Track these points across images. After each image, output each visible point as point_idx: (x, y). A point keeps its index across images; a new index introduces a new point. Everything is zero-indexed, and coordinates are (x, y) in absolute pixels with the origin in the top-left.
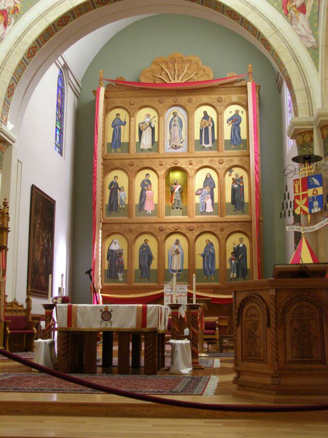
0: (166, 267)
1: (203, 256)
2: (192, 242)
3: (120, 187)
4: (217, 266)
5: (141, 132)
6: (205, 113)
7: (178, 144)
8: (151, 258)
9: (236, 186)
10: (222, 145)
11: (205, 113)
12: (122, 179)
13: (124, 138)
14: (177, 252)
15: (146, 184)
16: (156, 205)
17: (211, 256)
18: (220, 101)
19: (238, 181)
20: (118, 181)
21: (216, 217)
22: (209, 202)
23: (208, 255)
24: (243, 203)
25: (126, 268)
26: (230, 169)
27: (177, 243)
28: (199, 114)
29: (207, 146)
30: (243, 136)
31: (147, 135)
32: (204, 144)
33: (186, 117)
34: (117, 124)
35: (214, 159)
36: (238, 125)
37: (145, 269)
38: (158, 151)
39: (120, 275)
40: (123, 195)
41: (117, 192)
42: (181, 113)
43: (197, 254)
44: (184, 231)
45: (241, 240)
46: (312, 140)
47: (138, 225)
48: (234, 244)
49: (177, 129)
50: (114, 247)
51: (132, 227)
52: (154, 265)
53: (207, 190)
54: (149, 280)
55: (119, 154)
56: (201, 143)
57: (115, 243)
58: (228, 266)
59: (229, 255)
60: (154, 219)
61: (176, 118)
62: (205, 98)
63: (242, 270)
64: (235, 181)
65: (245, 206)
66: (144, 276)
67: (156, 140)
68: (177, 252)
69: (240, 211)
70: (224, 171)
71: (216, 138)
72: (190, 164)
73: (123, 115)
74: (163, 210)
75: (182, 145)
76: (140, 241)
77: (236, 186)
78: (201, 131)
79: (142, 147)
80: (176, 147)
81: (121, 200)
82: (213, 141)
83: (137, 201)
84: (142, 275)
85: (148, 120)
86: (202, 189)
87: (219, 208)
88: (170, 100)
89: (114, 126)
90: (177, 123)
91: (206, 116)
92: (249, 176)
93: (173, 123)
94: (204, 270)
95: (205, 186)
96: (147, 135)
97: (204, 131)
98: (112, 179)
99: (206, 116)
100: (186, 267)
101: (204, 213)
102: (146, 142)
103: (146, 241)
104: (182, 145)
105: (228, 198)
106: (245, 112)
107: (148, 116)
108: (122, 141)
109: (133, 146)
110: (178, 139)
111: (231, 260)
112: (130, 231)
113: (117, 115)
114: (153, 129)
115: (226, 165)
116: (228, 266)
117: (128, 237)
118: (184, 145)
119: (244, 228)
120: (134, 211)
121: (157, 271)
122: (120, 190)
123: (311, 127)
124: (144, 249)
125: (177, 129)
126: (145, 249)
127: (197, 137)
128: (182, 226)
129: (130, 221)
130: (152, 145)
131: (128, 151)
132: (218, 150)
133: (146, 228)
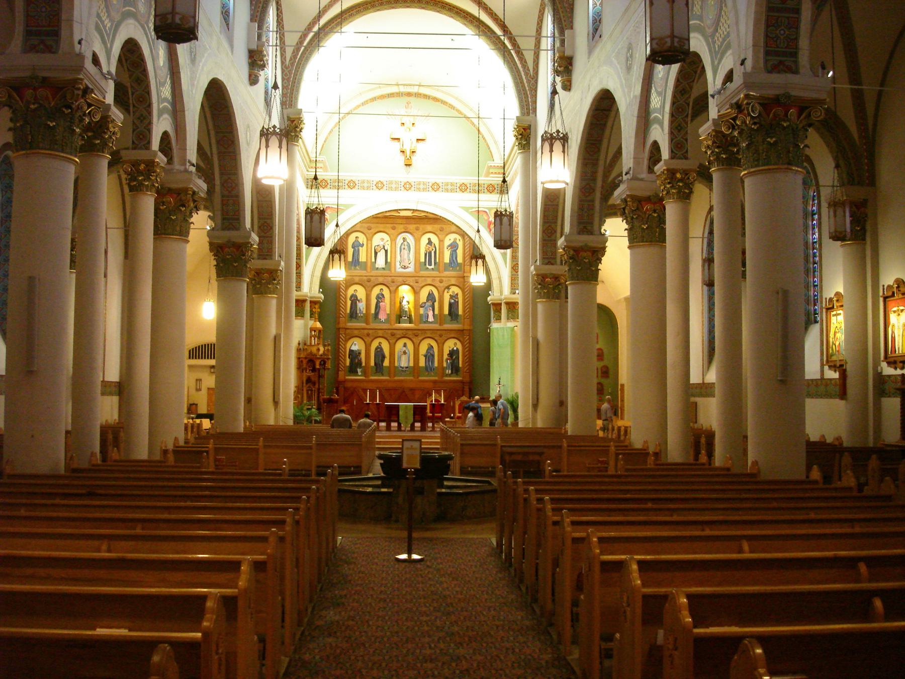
0: (396, 364)
1: (425, 356)
2: (416, 346)
3: (359, 298)
4: (436, 364)
5: (376, 253)
6: (429, 239)
7: (407, 265)
8: (384, 357)
9: (453, 301)
10: (442, 267)
11: (429, 239)
13: (363, 258)
14: (405, 353)
15: (380, 297)
16: (388, 314)
17: (431, 357)
18: (442, 230)
19: (454, 297)
20: (357, 294)
21: (437, 326)
22: (431, 313)
23: (429, 356)
24: (457, 315)
25: (364, 364)
26: (448, 288)
27: (405, 345)
28: (424, 240)
29: (430, 267)
30: (460, 260)
31: (381, 256)
32: (428, 266)
33: (413, 242)
34: (357, 246)
35: (436, 279)
36: (455, 251)
37: (379, 366)
38: (390, 270)
39: (359, 370)
40: (361, 306)
41: (356, 303)
43: (420, 354)
44: (410, 337)
45: (455, 344)
46: (501, 309)
47: (374, 331)
48: (450, 347)
49: (405, 252)
50: (354, 348)
51: (371, 332)
52: (386, 363)
53: (430, 303)
54: (383, 375)
56: (426, 265)
57: (355, 344)
58: (445, 365)
59: (445, 356)
61: (405, 243)
62: (429, 228)
63: (455, 369)
64: (451, 297)
65: (459, 318)
66: (378, 371)
67: (389, 260)
68: (405, 353)
69: (455, 322)
70: (443, 289)
71: (437, 261)
72: (417, 282)
73: (362, 239)
74: (393, 318)
75: (410, 265)
76: (375, 345)
77: (453, 301)
78: (426, 255)
79: (377, 266)
80: (405, 268)
81: (360, 310)
82: (435, 263)
83: (373, 311)
84: (376, 370)
85: (381, 243)
86: (425, 303)
87: (439, 318)
88: (400, 228)
89: (353, 247)
90: (406, 247)
91: (430, 242)
93: (403, 247)
94: (426, 368)
95: (428, 300)
96: (381, 256)
97: (428, 255)
98: (353, 292)
99: (430, 242)
100: (411, 364)
101: (427, 322)
102: (381, 262)
103: (380, 343)
104: (410, 265)
105: (446, 311)
106: (461, 240)
107: (382, 239)
108: (360, 260)
109: (369, 264)
110: (407, 261)
111: (447, 359)
112: (368, 335)
113: (356, 237)
114: (386, 251)
115: (445, 284)
116: (445, 365)
117: (366, 340)
119: (459, 334)
120: (371, 319)
121: (389, 367)
122: (359, 301)
123: (500, 302)
124: (379, 350)
125: (405, 252)
127: (422, 260)
128: (410, 332)
129: (368, 327)
130: (386, 264)
131: (366, 269)
132: (439, 271)
133: (380, 333)
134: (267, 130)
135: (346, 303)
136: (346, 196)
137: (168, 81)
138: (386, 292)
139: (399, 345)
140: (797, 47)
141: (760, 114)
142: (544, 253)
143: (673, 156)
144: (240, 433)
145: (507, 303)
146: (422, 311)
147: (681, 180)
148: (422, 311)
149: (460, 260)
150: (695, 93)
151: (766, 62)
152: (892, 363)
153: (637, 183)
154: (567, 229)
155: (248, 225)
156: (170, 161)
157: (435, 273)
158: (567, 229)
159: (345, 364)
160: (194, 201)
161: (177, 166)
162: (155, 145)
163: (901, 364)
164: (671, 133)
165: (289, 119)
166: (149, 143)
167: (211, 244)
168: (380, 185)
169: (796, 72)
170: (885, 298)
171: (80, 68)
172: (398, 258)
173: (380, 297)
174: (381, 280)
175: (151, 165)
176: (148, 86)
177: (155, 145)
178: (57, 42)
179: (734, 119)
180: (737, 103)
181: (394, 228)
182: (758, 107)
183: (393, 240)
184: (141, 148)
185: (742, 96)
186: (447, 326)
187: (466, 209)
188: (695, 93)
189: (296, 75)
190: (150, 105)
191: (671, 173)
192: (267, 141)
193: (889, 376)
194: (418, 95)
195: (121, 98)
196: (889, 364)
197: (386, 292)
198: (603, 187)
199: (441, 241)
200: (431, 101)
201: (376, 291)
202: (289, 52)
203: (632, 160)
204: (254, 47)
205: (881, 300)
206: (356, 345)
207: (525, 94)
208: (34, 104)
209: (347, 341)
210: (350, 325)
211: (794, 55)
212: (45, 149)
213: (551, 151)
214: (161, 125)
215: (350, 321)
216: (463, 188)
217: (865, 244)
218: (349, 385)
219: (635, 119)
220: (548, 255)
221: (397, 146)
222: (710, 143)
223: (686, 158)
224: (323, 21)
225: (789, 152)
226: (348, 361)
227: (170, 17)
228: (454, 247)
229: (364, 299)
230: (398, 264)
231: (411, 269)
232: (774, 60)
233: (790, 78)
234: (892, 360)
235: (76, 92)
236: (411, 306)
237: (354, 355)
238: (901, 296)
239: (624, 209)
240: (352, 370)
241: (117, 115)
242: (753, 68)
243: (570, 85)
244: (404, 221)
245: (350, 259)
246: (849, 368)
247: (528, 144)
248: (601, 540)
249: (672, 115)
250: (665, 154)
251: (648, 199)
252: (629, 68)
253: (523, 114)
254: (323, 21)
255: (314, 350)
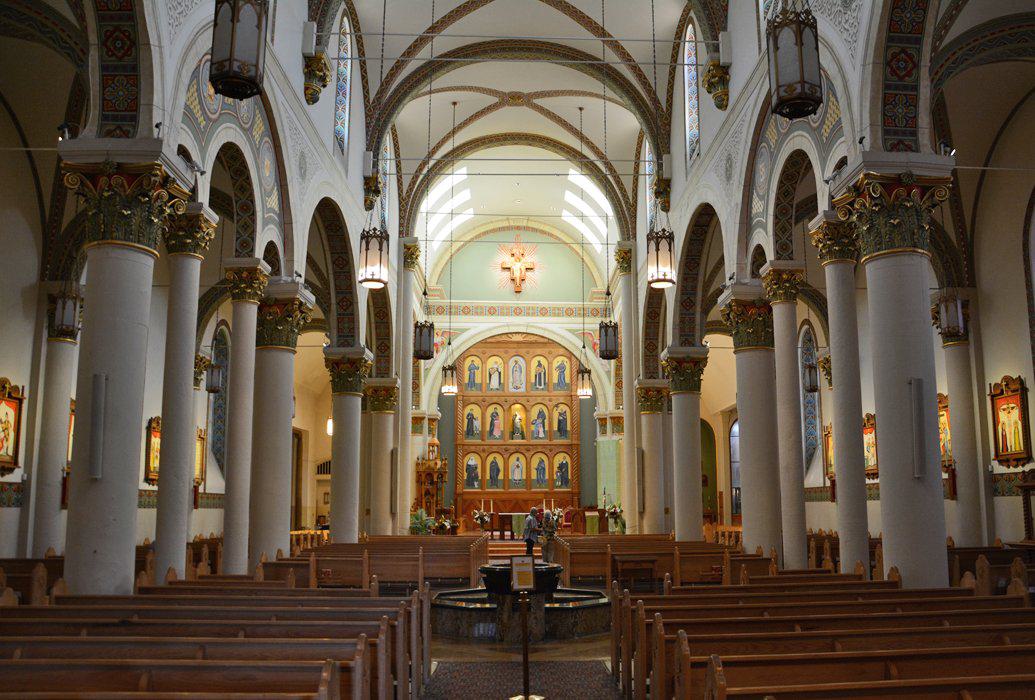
4: (547, 477)
5: (490, 376)
7: (519, 385)
8: (498, 470)
10: (551, 387)
12: (476, 411)
13: (478, 380)
15: (494, 416)
18: (550, 353)
21: (546, 441)
22: (541, 430)
23: (541, 469)
26: (557, 406)
27: (518, 460)
30: (568, 380)
31: (495, 377)
34: (472, 369)
37: (494, 480)
39: (476, 484)
40: (477, 424)
42: (521, 361)
45: (564, 458)
49: (518, 374)
50: (471, 463)
52: (501, 476)
53: (540, 421)
55: (473, 392)
59: (556, 469)
60: (501, 442)
62: (539, 351)
63: (565, 481)
64: (560, 414)
73: (477, 362)
74: (507, 435)
76: (490, 459)
80: (517, 388)
83: (488, 429)
87: (549, 434)
88: (512, 352)
91: (540, 365)
92: (571, 410)
96: (495, 377)
97: (538, 376)
99: (540, 365)
100: (524, 477)
102: (495, 383)
105: (555, 428)
107: (496, 363)
112: (484, 451)
116: (555, 477)
118: (524, 386)
119: (568, 449)
120: (487, 435)
125: (518, 374)
126: (494, 465)
128: (522, 447)
131: (481, 390)
134: (368, 232)
135: (463, 420)
136: (459, 322)
137: (275, 193)
138: (500, 410)
139: (513, 460)
140: (916, 126)
141: (881, 195)
142: (646, 367)
143: (778, 256)
144: (353, 545)
145: (611, 418)
146: (533, 428)
147: (787, 281)
148: (533, 428)
149: (568, 380)
150: (800, 196)
151: (885, 141)
152: (1004, 461)
153: (740, 289)
154: (669, 341)
155: (363, 342)
156: (276, 271)
157: (546, 393)
158: (669, 341)
159: (463, 477)
160: (302, 312)
161: (284, 277)
162: (259, 252)
163: (1015, 463)
164: (776, 235)
165: (406, 247)
166: (253, 250)
167: (327, 360)
168: (492, 311)
169: (917, 150)
170: (993, 397)
171: (158, 153)
172: (511, 380)
173: (494, 416)
174: (495, 400)
175: (253, 272)
176: (252, 194)
177: (259, 252)
178: (135, 127)
179: (852, 204)
180: (854, 186)
181: (506, 352)
182: (879, 189)
183: (506, 363)
184: (244, 256)
185: (862, 176)
186: (556, 442)
187: (572, 331)
188: (800, 196)
189: (412, 206)
190: (254, 214)
191: (777, 273)
192: (367, 244)
193: (1002, 475)
194: (527, 228)
195: (218, 200)
196: (1001, 462)
197: (500, 410)
198: (703, 300)
199: (550, 364)
200: (538, 234)
201: (491, 410)
202: (405, 188)
203: (735, 266)
204: (370, 174)
205: (988, 399)
206: (473, 460)
207: (626, 220)
208: (108, 191)
209: (464, 456)
210: (468, 441)
211: (914, 134)
212: (119, 239)
213: (658, 250)
214: (266, 235)
215: (466, 438)
216: (570, 312)
217: (969, 344)
218: (465, 497)
219: (737, 226)
220: (651, 370)
221: (507, 274)
222: (821, 236)
223: (792, 259)
224: (438, 155)
225: (914, 234)
226: (466, 474)
227: (227, 63)
228: (561, 368)
229: (480, 418)
230: (511, 386)
231: (522, 390)
232: (893, 139)
233: (912, 156)
234: (1004, 458)
235: (153, 179)
236: (523, 423)
237: (471, 469)
238: (1010, 393)
239: (728, 315)
240: (470, 483)
241: (212, 217)
242: (872, 146)
243: (669, 206)
244: (515, 345)
245: (467, 381)
246: (958, 468)
247: (630, 266)
248: (726, 664)
249: (776, 217)
250: (770, 255)
251: (752, 304)
252: (729, 177)
253: (624, 239)
254: (438, 155)
255: (432, 464)
